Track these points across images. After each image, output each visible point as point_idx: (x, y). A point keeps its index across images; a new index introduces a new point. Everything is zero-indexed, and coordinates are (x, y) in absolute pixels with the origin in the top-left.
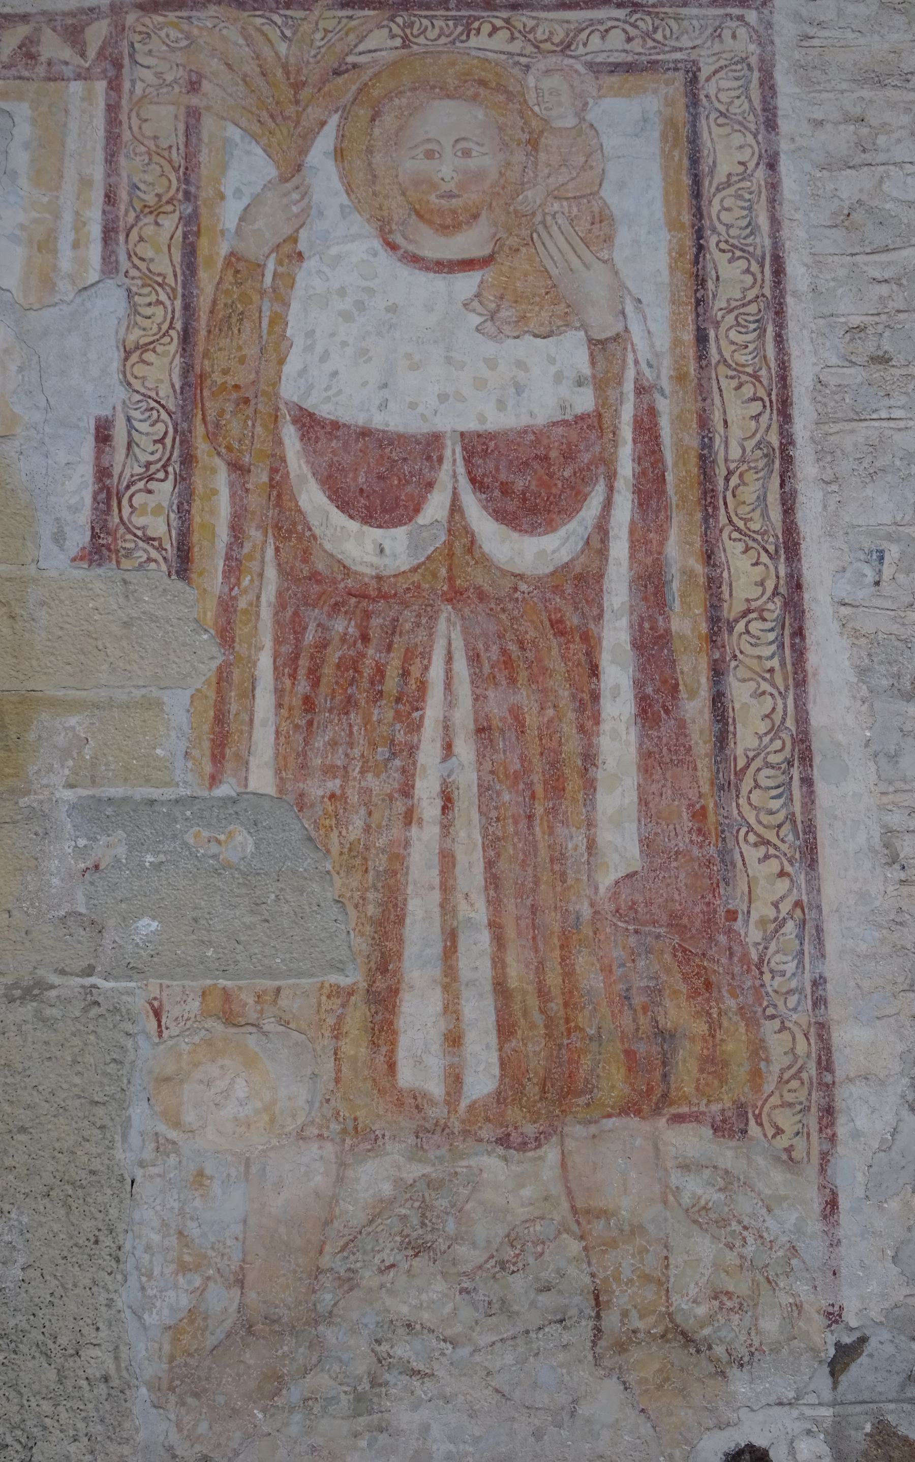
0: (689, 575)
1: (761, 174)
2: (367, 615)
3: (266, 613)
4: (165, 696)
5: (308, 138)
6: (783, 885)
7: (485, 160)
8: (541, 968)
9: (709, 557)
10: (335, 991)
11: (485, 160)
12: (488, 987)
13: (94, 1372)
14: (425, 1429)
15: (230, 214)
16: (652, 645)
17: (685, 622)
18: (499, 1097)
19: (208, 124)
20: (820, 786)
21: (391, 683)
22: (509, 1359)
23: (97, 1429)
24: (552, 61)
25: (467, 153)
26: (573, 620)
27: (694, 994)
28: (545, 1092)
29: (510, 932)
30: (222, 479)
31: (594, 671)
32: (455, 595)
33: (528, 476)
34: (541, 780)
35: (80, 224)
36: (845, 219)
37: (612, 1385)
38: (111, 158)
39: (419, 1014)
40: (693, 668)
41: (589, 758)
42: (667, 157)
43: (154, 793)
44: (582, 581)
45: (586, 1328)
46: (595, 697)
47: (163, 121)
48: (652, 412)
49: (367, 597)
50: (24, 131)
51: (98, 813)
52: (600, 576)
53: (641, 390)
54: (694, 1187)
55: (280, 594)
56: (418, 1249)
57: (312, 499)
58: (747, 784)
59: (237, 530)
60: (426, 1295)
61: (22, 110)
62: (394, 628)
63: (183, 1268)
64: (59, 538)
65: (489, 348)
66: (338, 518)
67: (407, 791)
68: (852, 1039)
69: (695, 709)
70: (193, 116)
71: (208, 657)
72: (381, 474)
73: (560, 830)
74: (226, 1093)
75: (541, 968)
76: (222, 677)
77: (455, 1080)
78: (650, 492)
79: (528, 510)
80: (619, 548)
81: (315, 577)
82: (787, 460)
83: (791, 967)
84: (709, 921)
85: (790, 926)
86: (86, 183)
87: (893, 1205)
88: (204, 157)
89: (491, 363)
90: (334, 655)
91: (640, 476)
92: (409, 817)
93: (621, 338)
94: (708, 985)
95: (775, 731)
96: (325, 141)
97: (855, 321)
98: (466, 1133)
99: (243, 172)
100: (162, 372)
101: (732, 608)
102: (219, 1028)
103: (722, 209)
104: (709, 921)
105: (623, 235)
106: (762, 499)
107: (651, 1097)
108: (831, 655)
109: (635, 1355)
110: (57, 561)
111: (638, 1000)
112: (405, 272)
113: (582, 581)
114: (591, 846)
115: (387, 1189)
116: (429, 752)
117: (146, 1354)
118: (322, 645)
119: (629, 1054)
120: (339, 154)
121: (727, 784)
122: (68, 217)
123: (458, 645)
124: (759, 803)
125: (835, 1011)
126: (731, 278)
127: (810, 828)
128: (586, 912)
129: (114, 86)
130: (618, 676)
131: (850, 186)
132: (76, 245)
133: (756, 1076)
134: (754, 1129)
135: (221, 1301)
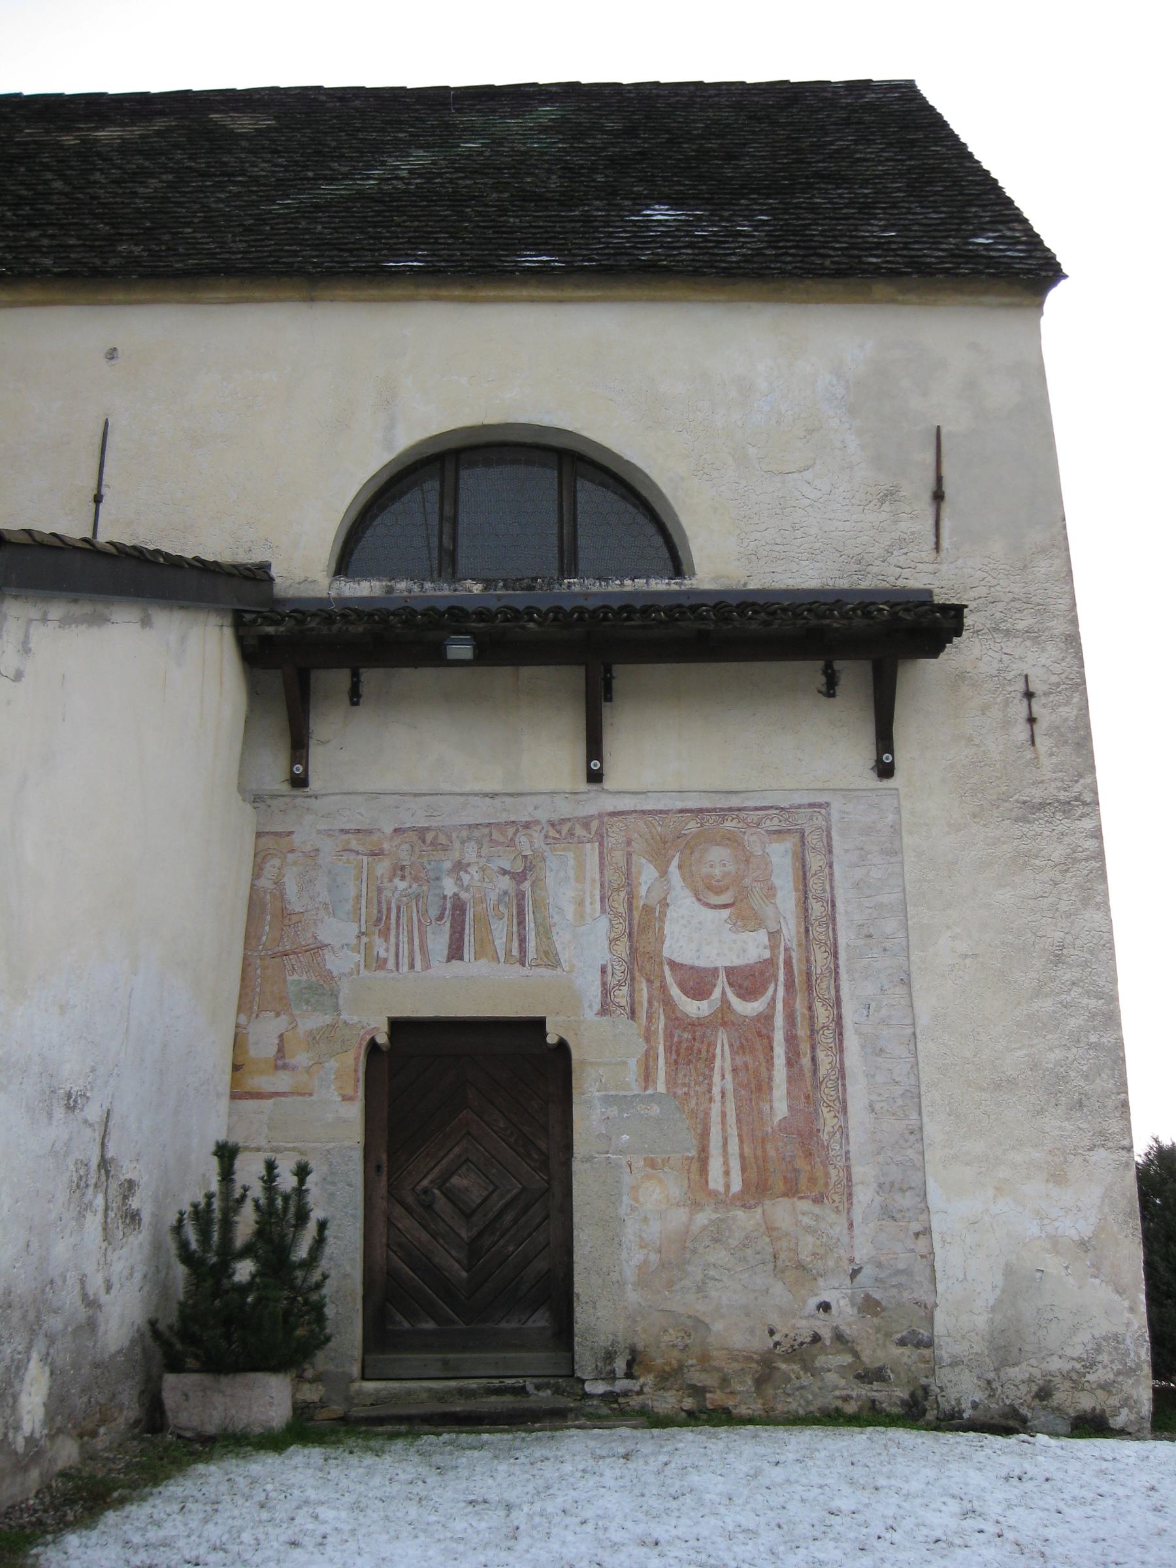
0: (803, 1015)
1: (827, 870)
2: (695, 1032)
3: (661, 1031)
4: (629, 1061)
5: (669, 862)
6: (836, 1120)
7: (731, 868)
8: (755, 1148)
9: (810, 1008)
10: (688, 1158)
11: (731, 868)
12: (737, 1156)
13: (614, 1279)
14: (720, 1297)
15: (643, 890)
16: (791, 1040)
17: (802, 1032)
18: (742, 1191)
19: (634, 857)
20: (848, 1086)
21: (704, 1054)
22: (746, 1275)
23: (615, 1297)
24: (753, 830)
25: (724, 865)
26: (764, 1032)
27: (806, 1157)
28: (758, 1188)
29: (745, 1137)
30: (644, 985)
31: (772, 1049)
32: (724, 1024)
33: (749, 981)
35: (592, 896)
36: (857, 885)
37: (780, 1284)
38: (602, 871)
40: (805, 1047)
41: (770, 1079)
42: (794, 864)
43: (626, 1093)
44: (766, 1018)
45: (771, 1265)
46: (772, 1058)
47: (619, 857)
48: (790, 957)
49: (694, 1025)
50: (571, 862)
51: (608, 1100)
52: (773, 1016)
53: (786, 950)
54: (806, 1220)
55: (665, 1025)
56: (716, 1240)
57: (675, 991)
58: (824, 1086)
59: (650, 1002)
60: (720, 1255)
61: (571, 855)
62: (704, 1036)
63: (642, 1247)
64: (590, 1007)
65: (734, 936)
66: (684, 997)
67: (710, 1091)
68: (858, 1171)
69: (806, 1061)
70: (629, 854)
71: (643, 1046)
72: (698, 982)
73: (761, 1103)
74: (653, 1192)
75: (755, 1148)
76: (647, 1055)
77: (727, 1186)
78: (790, 986)
79: (748, 994)
80: (779, 1006)
81: (677, 1019)
82: (837, 973)
83: (838, 1148)
84: (811, 1132)
85: (838, 1135)
86: (594, 880)
87: (872, 1225)
88: (633, 870)
89: (735, 942)
90: (684, 1045)
91: (786, 980)
92: (711, 1100)
93: (779, 932)
94: (810, 1154)
95: (833, 1068)
96: (675, 862)
97: (860, 922)
98: (731, 1204)
99: (647, 874)
100: (623, 948)
101: (818, 1026)
102: (650, 1170)
103: (814, 884)
104: (811, 1132)
105: (779, 894)
106: (828, 988)
107: (792, 1190)
108: (852, 1042)
109: (787, 1274)
110: (590, 1014)
111: (788, 1159)
112: (704, 909)
113: (766, 1018)
114: (771, 1107)
115: (706, 1222)
116: (716, 1078)
117: (630, 1274)
118: (680, 1042)
119: (785, 1177)
120: (680, 867)
121: (817, 1086)
122: (588, 894)
123: (725, 1041)
124: (828, 1092)
125: (852, 1162)
127: (845, 1101)
128: (770, 1130)
129: (601, 845)
130: (779, 1051)
131: (858, 873)
132: (591, 904)
133: (827, 1184)
134: (826, 1201)
135: (654, 1257)
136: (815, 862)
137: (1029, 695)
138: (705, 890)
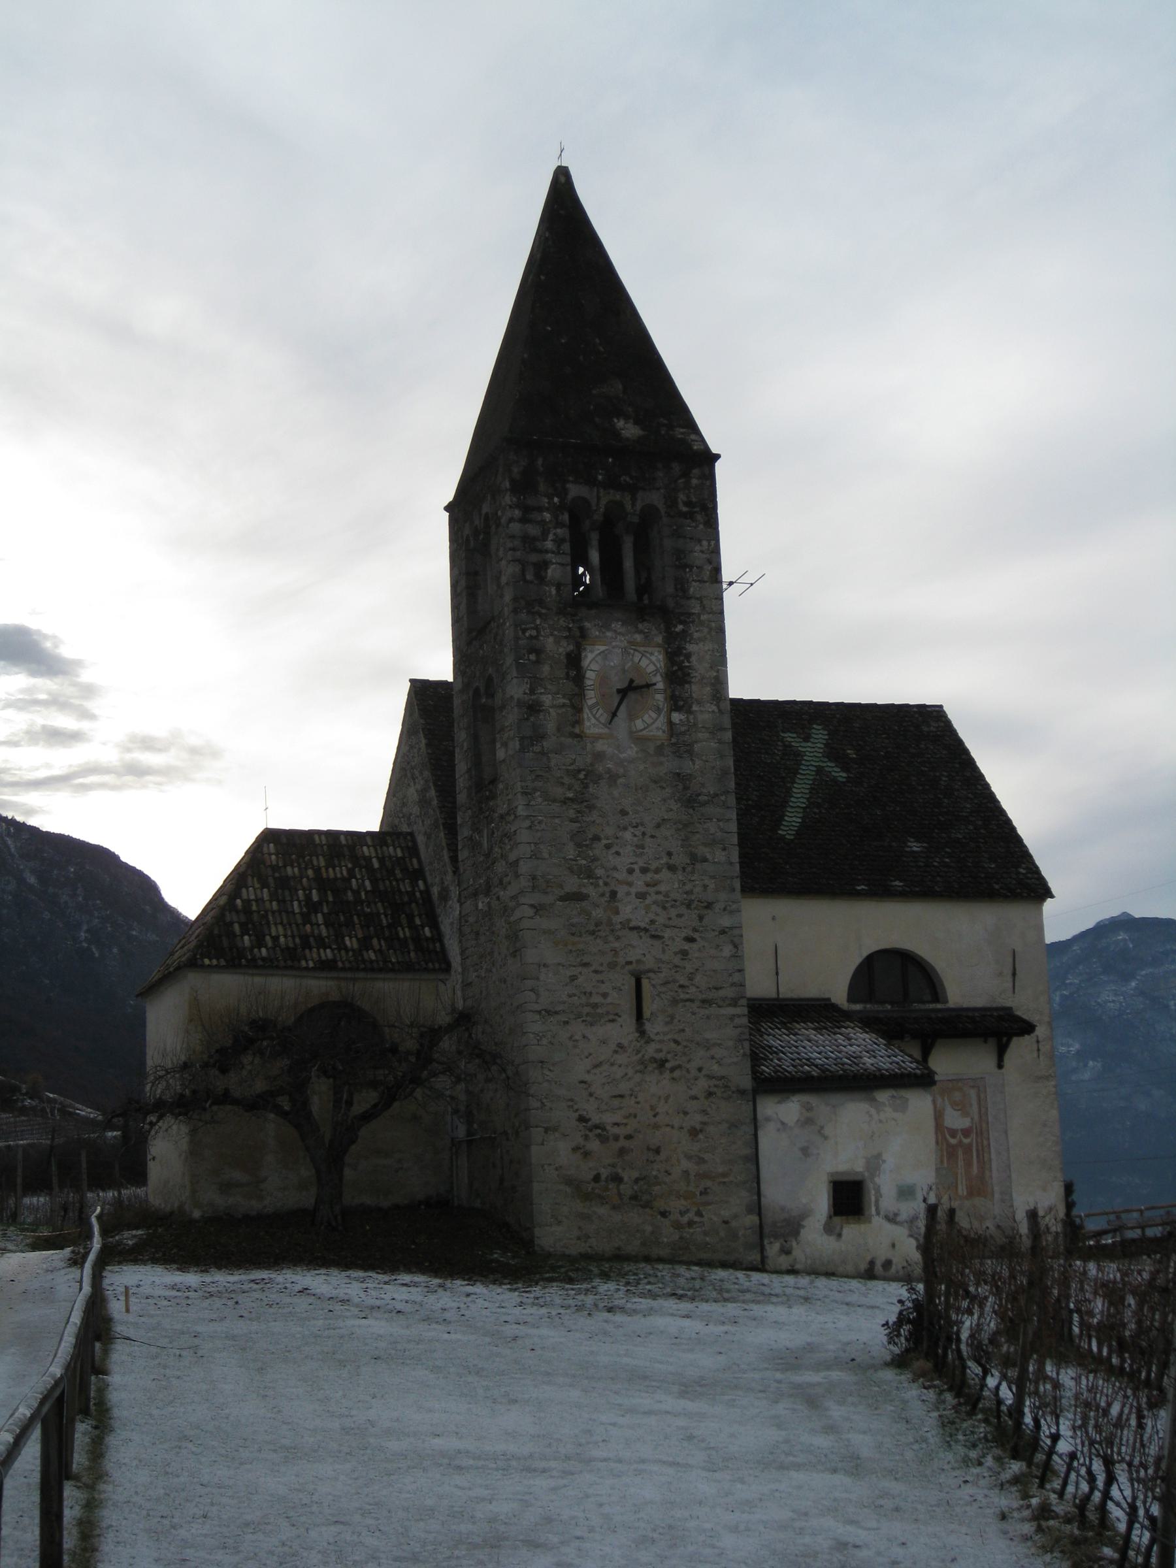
16: (977, 1150)
28: (971, 1194)
33: (966, 1132)
34: (968, 1164)
39: (960, 1187)
72: (953, 1133)
108: (993, 1150)
113: (970, 1145)
126: (983, 1110)
136: (982, 1096)
137: (1038, 1042)
138: (954, 1105)
